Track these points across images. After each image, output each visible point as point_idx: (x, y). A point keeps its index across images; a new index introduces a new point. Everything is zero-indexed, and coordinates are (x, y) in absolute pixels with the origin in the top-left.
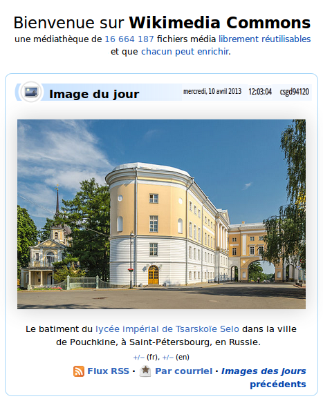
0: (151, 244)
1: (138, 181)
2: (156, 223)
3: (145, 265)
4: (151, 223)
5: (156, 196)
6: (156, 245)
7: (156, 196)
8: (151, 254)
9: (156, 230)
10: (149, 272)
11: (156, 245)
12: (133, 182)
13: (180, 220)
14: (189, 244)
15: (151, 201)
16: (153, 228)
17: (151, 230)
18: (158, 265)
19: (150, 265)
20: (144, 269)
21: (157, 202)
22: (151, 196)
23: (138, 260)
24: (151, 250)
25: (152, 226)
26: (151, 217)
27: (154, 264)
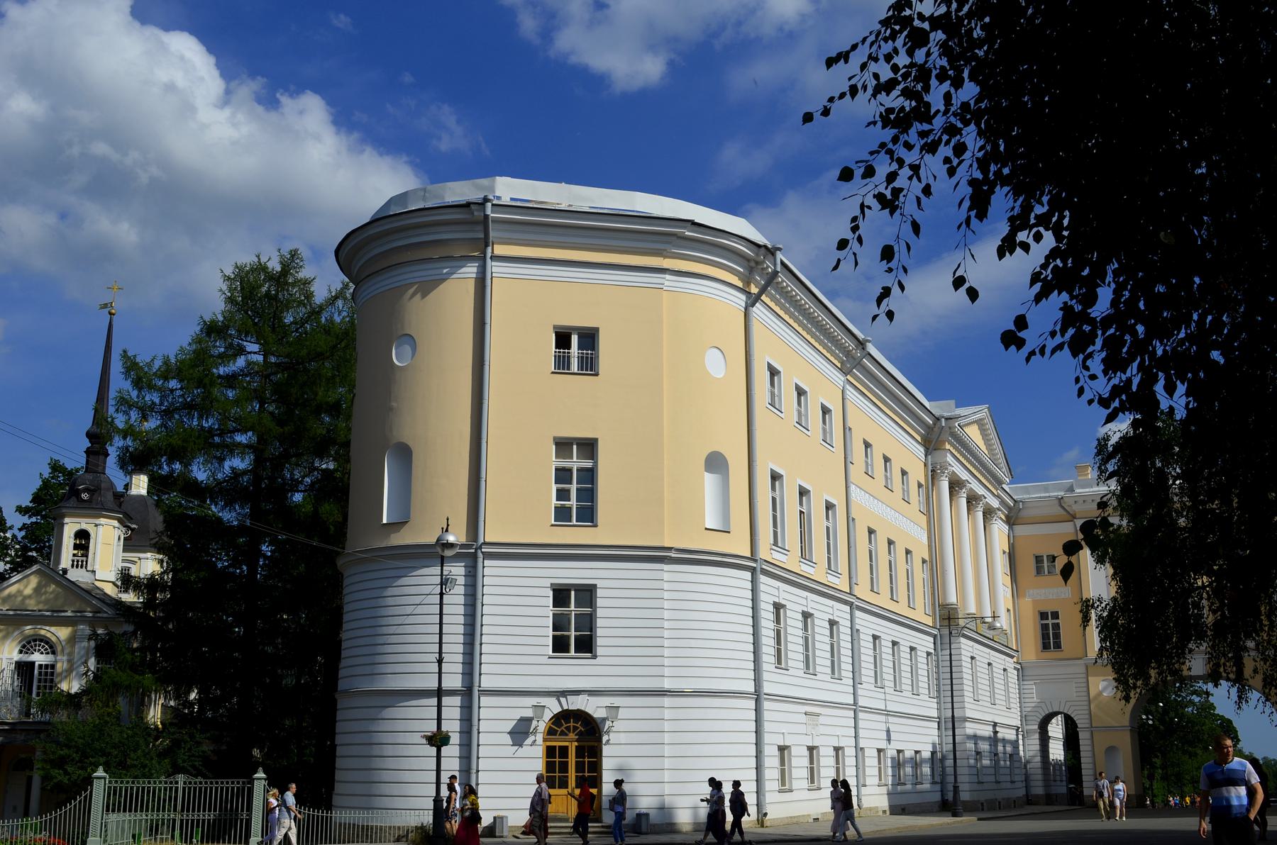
0: (561, 595)
1: (495, 268)
2: (589, 476)
3: (524, 708)
4: (563, 475)
5: (589, 338)
6: (587, 593)
7: (589, 338)
8: (560, 645)
9: (588, 515)
10: (550, 751)
11: (587, 593)
12: (471, 270)
13: (716, 463)
14: (771, 590)
15: (562, 364)
16: (573, 502)
17: (562, 515)
18: (595, 707)
19: (553, 707)
20: (520, 732)
21: (589, 365)
22: (563, 339)
23: (487, 682)
24: (559, 624)
25: (562, 495)
26: (563, 446)
27: (576, 703)
